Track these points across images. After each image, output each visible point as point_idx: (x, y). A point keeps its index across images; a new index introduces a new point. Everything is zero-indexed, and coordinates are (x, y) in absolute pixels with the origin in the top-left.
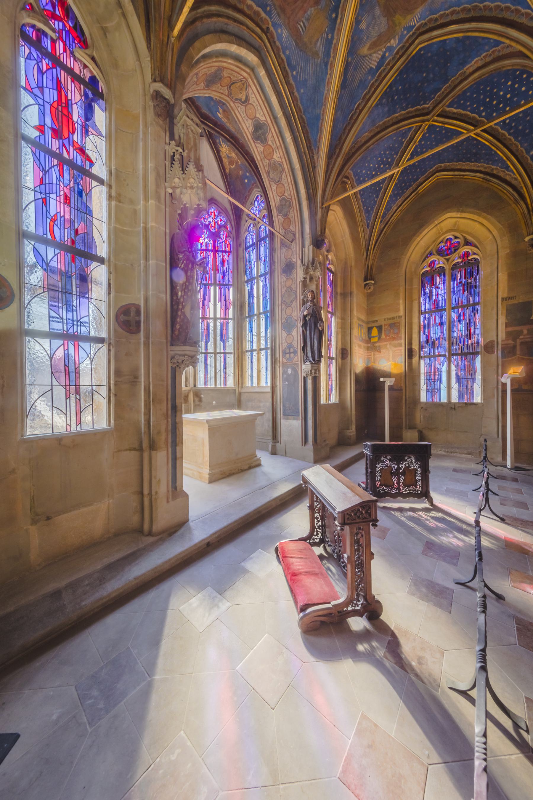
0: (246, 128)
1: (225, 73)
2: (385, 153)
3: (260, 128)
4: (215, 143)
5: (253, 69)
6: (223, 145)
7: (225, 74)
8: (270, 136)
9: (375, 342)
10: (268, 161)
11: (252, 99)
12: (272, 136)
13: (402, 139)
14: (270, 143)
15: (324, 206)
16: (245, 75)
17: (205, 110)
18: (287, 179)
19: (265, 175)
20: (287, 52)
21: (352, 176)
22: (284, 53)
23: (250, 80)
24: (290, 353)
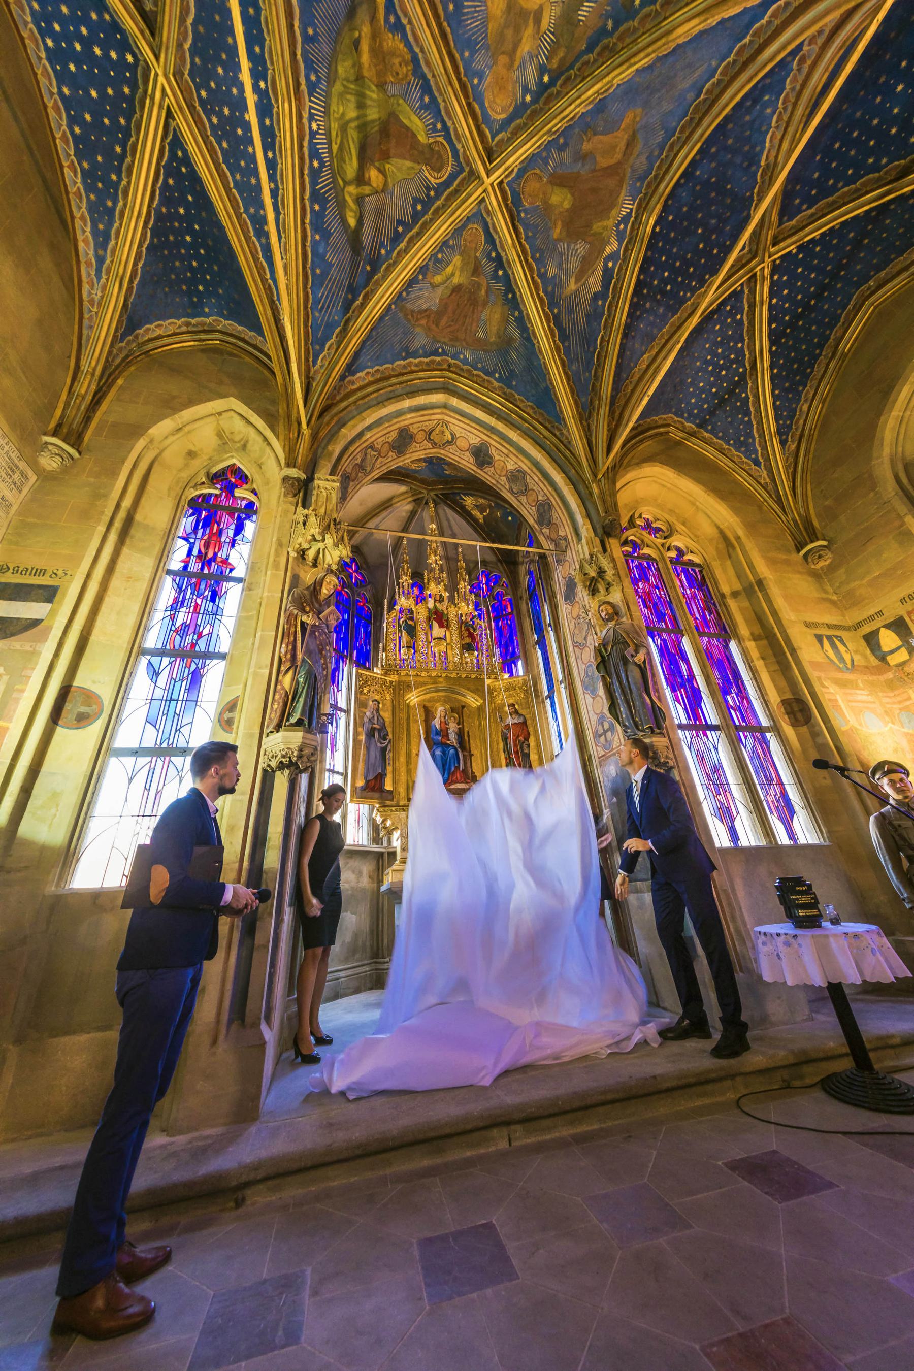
0: (467, 462)
1: (412, 430)
2: (714, 354)
3: (481, 451)
5: (445, 406)
7: (414, 429)
8: (493, 452)
9: (903, 664)
10: (504, 478)
11: (458, 432)
13: (733, 317)
19: (509, 494)
20: (480, 365)
21: (676, 419)
23: (446, 418)
24: (605, 732)
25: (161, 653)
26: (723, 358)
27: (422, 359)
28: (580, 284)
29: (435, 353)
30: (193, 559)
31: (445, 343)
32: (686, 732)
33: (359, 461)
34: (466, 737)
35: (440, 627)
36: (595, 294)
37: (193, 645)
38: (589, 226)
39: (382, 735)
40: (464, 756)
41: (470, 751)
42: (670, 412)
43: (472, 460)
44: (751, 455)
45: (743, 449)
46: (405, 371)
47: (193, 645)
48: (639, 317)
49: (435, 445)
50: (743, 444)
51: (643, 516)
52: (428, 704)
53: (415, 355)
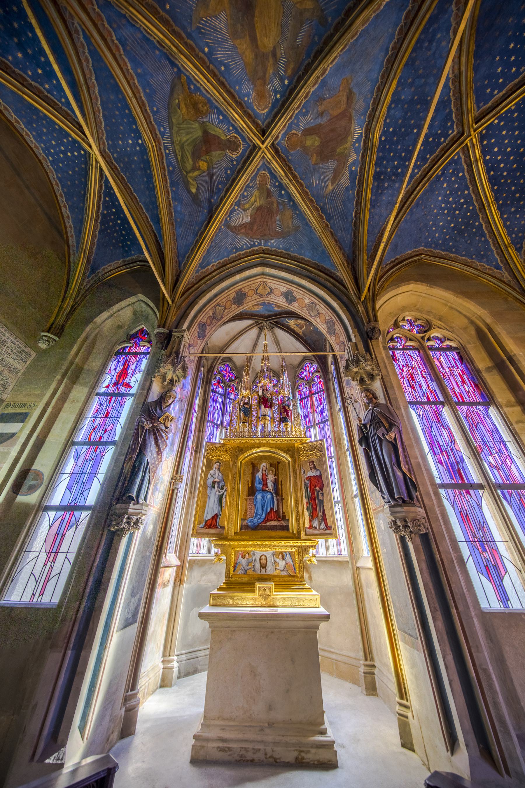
0: (282, 302)
4: (283, 325)
5: (263, 274)
6: (290, 321)
7: (246, 290)
11: (273, 286)
12: (298, 293)
13: (457, 176)
14: (298, 297)
15: (363, 299)
17: (267, 313)
20: (281, 246)
21: (426, 249)
26: (455, 203)
28: (335, 185)
29: (254, 245)
30: (112, 385)
32: (449, 491)
33: (211, 314)
34: (280, 486)
35: (265, 407)
36: (347, 188)
38: (334, 150)
39: (220, 486)
40: (277, 500)
41: (282, 496)
42: (420, 246)
44: (492, 263)
45: (485, 260)
48: (381, 193)
49: (261, 296)
50: (483, 256)
51: (406, 318)
52: (255, 462)
53: (241, 249)
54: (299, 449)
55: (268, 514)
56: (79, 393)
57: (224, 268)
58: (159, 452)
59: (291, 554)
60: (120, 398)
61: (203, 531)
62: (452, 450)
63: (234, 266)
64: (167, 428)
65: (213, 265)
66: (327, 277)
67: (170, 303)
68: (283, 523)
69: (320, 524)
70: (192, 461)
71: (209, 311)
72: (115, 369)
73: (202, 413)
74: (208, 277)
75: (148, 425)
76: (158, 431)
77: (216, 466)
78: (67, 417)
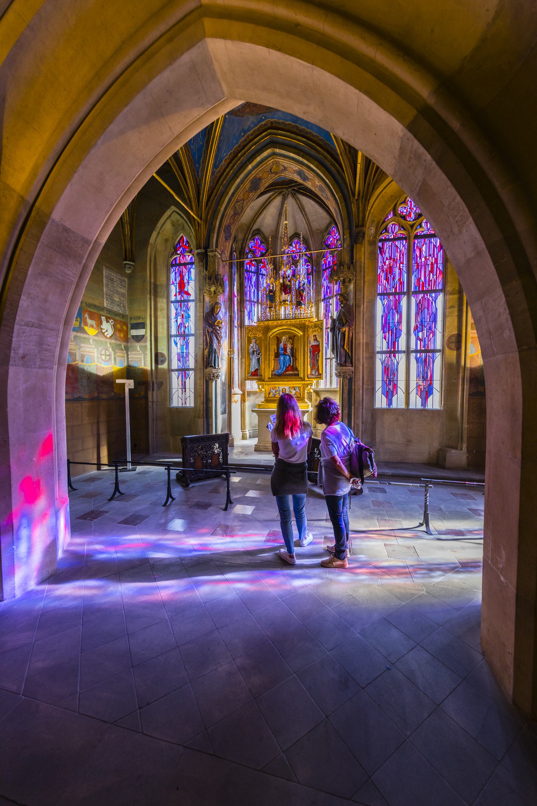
1: (258, 176)
11: (286, 165)
14: (310, 178)
16: (271, 161)
18: (329, 194)
20: (288, 118)
22: (287, 121)
25: (176, 336)
27: (255, 129)
29: (262, 120)
30: (178, 294)
31: (264, 113)
33: (232, 213)
35: (285, 294)
37: (184, 331)
43: (299, 177)
46: (246, 143)
47: (184, 331)
49: (276, 173)
53: (249, 130)
54: (308, 326)
55: (287, 368)
56: (162, 303)
57: (236, 159)
58: (219, 342)
59: (299, 388)
60: (186, 303)
61: (250, 377)
62: (396, 329)
63: (245, 153)
64: (220, 328)
65: (225, 160)
66: (333, 160)
67: (199, 221)
68: (296, 372)
69: (315, 373)
70: (239, 335)
71: (230, 212)
72: (176, 280)
73: (241, 296)
74: (222, 178)
75: (210, 330)
76: (216, 331)
77: (253, 341)
78: (162, 320)
